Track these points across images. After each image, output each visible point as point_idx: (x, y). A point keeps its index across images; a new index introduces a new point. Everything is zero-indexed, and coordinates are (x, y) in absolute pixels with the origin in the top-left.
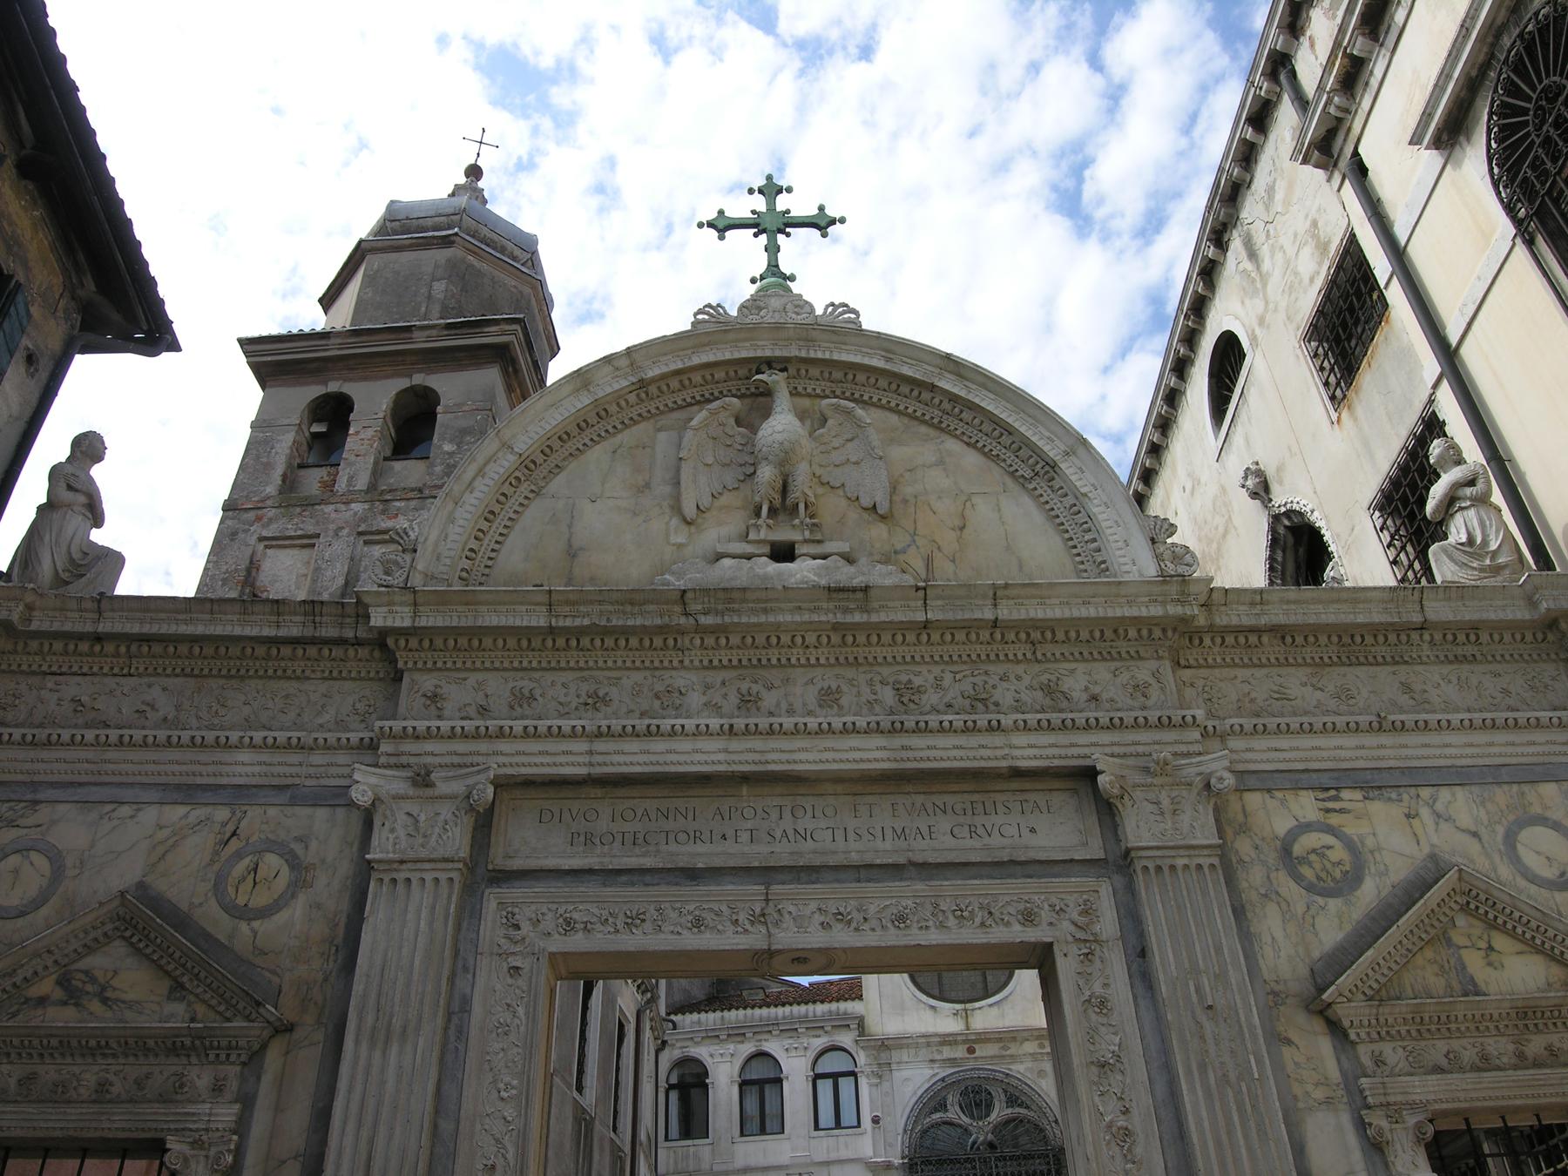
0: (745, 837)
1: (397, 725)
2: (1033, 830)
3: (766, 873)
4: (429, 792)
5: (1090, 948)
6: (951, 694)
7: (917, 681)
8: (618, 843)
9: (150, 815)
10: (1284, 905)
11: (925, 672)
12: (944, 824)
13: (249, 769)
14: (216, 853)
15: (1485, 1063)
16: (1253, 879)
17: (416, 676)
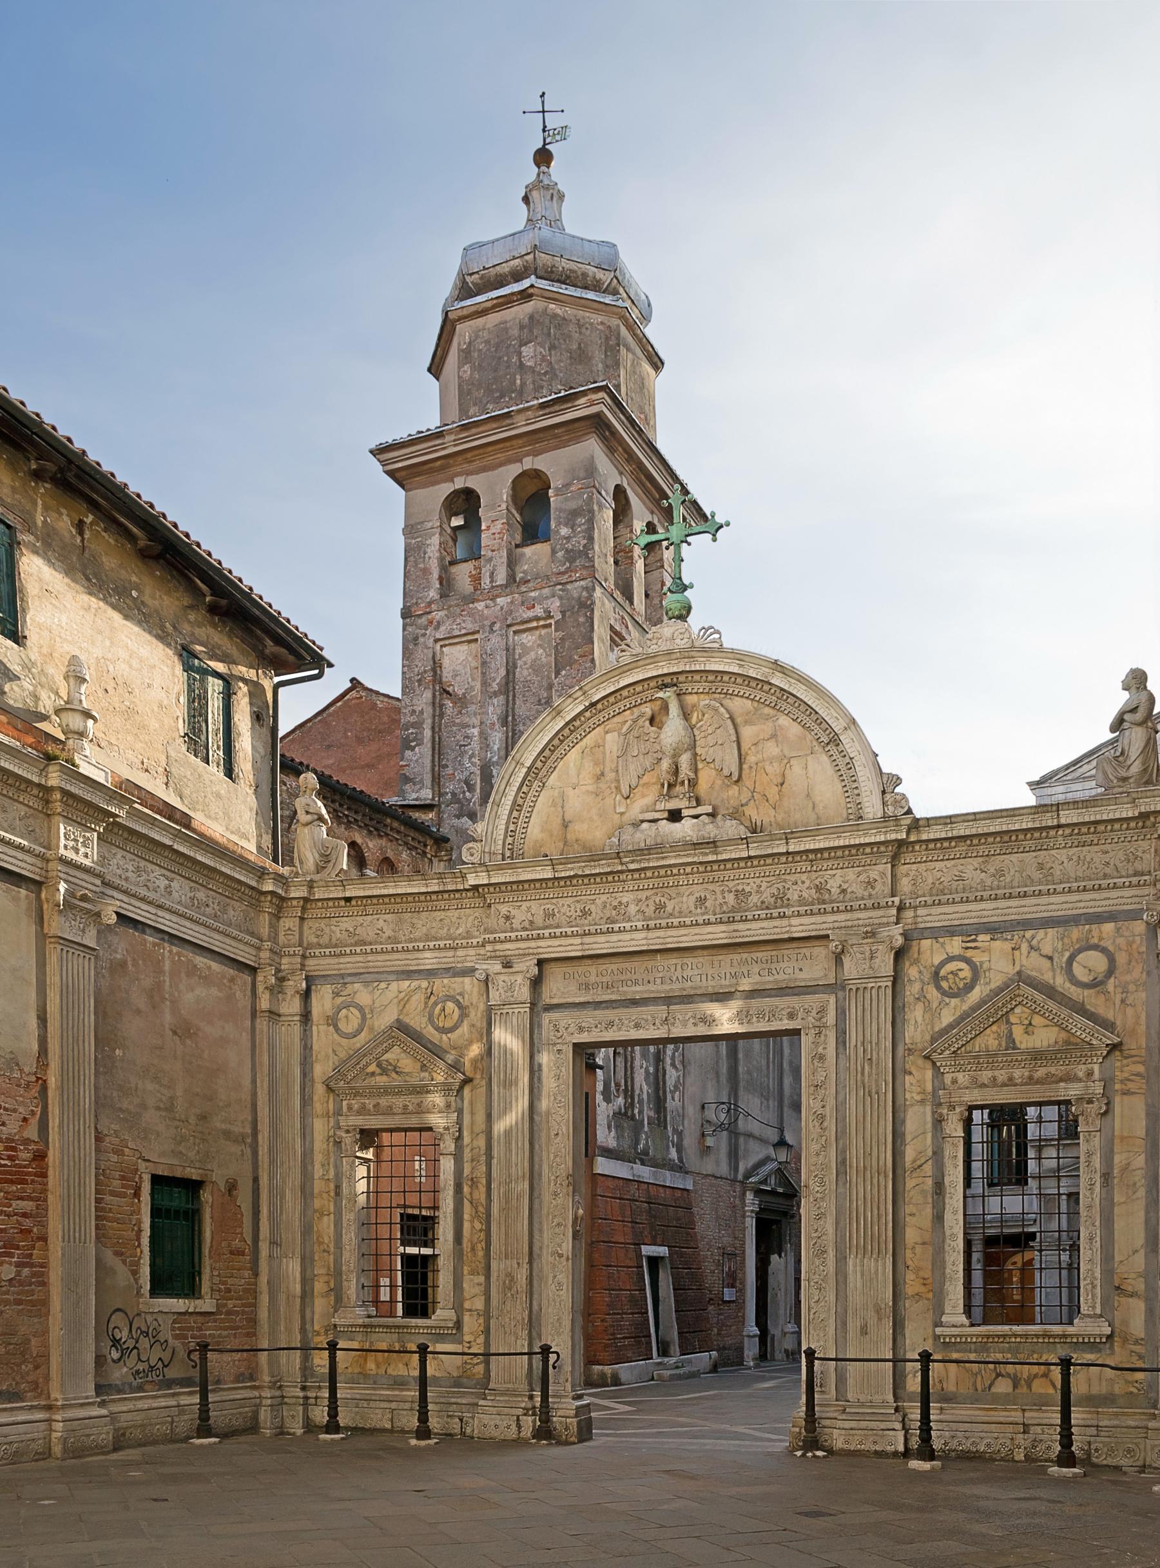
0: (659, 981)
1: (492, 937)
2: (801, 970)
3: (668, 1000)
4: (511, 970)
5: (820, 1030)
6: (765, 895)
7: (748, 889)
8: (600, 988)
9: (394, 986)
10: (927, 1004)
11: (752, 884)
12: (756, 969)
13: (431, 961)
14: (426, 1003)
15: (1011, 1082)
16: (911, 991)
17: (497, 906)
